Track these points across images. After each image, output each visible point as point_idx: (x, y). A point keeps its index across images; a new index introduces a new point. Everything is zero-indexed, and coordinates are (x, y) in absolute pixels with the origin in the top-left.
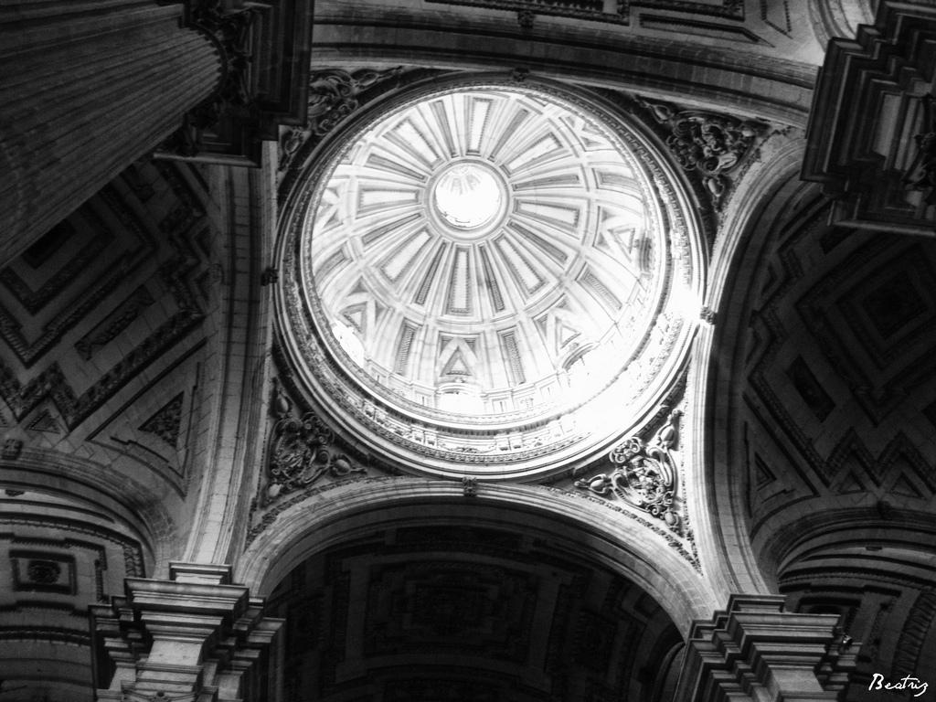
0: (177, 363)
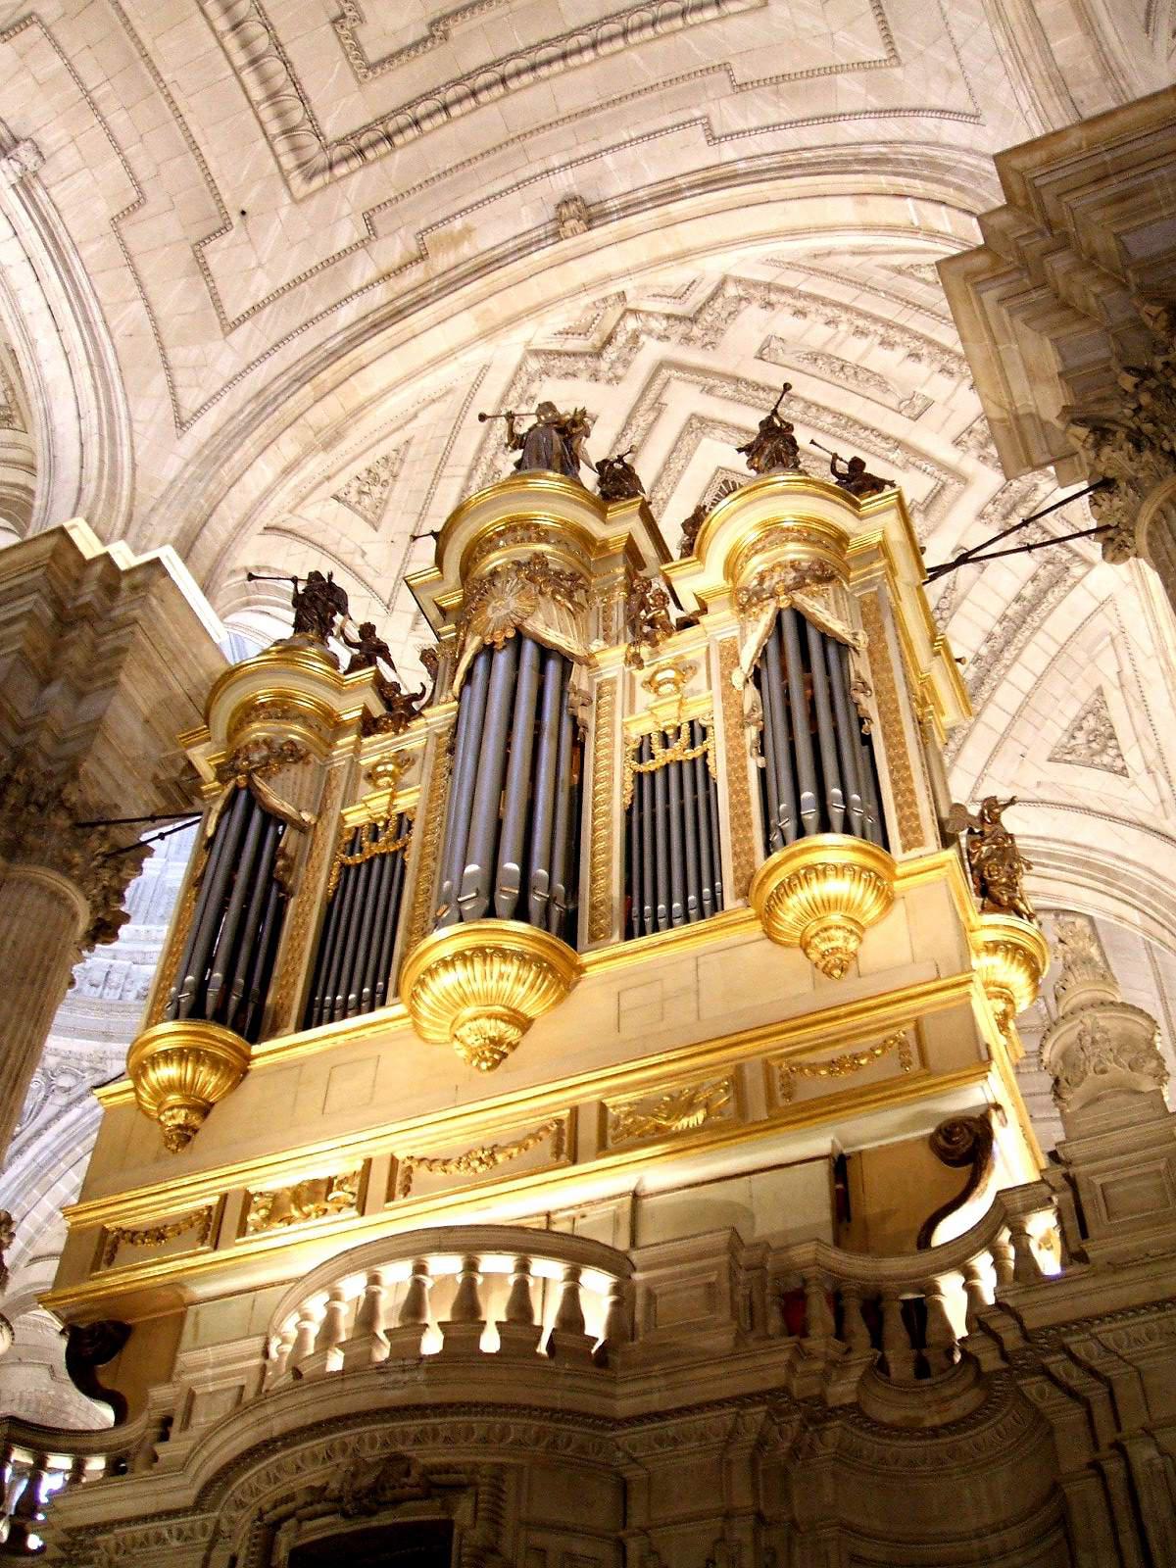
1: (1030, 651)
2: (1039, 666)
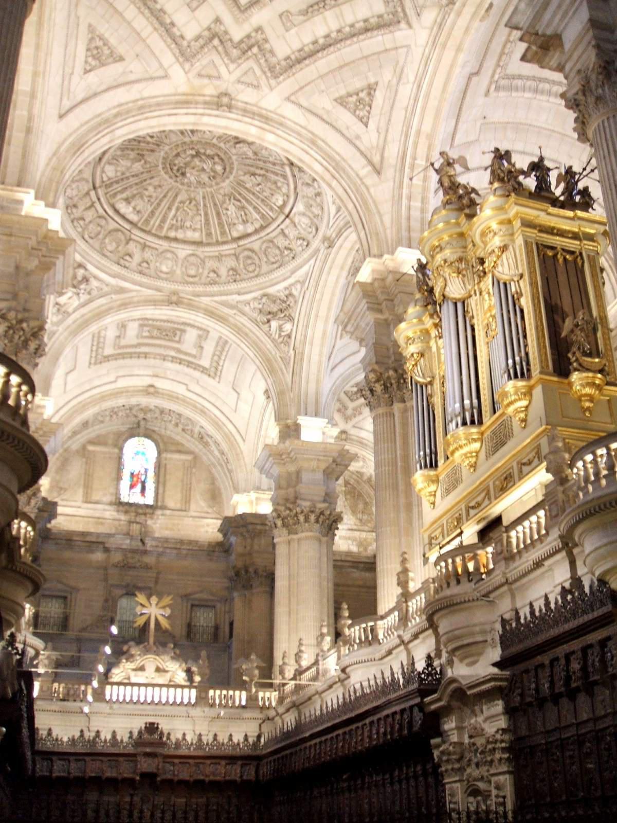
1: (144, 22)
2: (135, 24)
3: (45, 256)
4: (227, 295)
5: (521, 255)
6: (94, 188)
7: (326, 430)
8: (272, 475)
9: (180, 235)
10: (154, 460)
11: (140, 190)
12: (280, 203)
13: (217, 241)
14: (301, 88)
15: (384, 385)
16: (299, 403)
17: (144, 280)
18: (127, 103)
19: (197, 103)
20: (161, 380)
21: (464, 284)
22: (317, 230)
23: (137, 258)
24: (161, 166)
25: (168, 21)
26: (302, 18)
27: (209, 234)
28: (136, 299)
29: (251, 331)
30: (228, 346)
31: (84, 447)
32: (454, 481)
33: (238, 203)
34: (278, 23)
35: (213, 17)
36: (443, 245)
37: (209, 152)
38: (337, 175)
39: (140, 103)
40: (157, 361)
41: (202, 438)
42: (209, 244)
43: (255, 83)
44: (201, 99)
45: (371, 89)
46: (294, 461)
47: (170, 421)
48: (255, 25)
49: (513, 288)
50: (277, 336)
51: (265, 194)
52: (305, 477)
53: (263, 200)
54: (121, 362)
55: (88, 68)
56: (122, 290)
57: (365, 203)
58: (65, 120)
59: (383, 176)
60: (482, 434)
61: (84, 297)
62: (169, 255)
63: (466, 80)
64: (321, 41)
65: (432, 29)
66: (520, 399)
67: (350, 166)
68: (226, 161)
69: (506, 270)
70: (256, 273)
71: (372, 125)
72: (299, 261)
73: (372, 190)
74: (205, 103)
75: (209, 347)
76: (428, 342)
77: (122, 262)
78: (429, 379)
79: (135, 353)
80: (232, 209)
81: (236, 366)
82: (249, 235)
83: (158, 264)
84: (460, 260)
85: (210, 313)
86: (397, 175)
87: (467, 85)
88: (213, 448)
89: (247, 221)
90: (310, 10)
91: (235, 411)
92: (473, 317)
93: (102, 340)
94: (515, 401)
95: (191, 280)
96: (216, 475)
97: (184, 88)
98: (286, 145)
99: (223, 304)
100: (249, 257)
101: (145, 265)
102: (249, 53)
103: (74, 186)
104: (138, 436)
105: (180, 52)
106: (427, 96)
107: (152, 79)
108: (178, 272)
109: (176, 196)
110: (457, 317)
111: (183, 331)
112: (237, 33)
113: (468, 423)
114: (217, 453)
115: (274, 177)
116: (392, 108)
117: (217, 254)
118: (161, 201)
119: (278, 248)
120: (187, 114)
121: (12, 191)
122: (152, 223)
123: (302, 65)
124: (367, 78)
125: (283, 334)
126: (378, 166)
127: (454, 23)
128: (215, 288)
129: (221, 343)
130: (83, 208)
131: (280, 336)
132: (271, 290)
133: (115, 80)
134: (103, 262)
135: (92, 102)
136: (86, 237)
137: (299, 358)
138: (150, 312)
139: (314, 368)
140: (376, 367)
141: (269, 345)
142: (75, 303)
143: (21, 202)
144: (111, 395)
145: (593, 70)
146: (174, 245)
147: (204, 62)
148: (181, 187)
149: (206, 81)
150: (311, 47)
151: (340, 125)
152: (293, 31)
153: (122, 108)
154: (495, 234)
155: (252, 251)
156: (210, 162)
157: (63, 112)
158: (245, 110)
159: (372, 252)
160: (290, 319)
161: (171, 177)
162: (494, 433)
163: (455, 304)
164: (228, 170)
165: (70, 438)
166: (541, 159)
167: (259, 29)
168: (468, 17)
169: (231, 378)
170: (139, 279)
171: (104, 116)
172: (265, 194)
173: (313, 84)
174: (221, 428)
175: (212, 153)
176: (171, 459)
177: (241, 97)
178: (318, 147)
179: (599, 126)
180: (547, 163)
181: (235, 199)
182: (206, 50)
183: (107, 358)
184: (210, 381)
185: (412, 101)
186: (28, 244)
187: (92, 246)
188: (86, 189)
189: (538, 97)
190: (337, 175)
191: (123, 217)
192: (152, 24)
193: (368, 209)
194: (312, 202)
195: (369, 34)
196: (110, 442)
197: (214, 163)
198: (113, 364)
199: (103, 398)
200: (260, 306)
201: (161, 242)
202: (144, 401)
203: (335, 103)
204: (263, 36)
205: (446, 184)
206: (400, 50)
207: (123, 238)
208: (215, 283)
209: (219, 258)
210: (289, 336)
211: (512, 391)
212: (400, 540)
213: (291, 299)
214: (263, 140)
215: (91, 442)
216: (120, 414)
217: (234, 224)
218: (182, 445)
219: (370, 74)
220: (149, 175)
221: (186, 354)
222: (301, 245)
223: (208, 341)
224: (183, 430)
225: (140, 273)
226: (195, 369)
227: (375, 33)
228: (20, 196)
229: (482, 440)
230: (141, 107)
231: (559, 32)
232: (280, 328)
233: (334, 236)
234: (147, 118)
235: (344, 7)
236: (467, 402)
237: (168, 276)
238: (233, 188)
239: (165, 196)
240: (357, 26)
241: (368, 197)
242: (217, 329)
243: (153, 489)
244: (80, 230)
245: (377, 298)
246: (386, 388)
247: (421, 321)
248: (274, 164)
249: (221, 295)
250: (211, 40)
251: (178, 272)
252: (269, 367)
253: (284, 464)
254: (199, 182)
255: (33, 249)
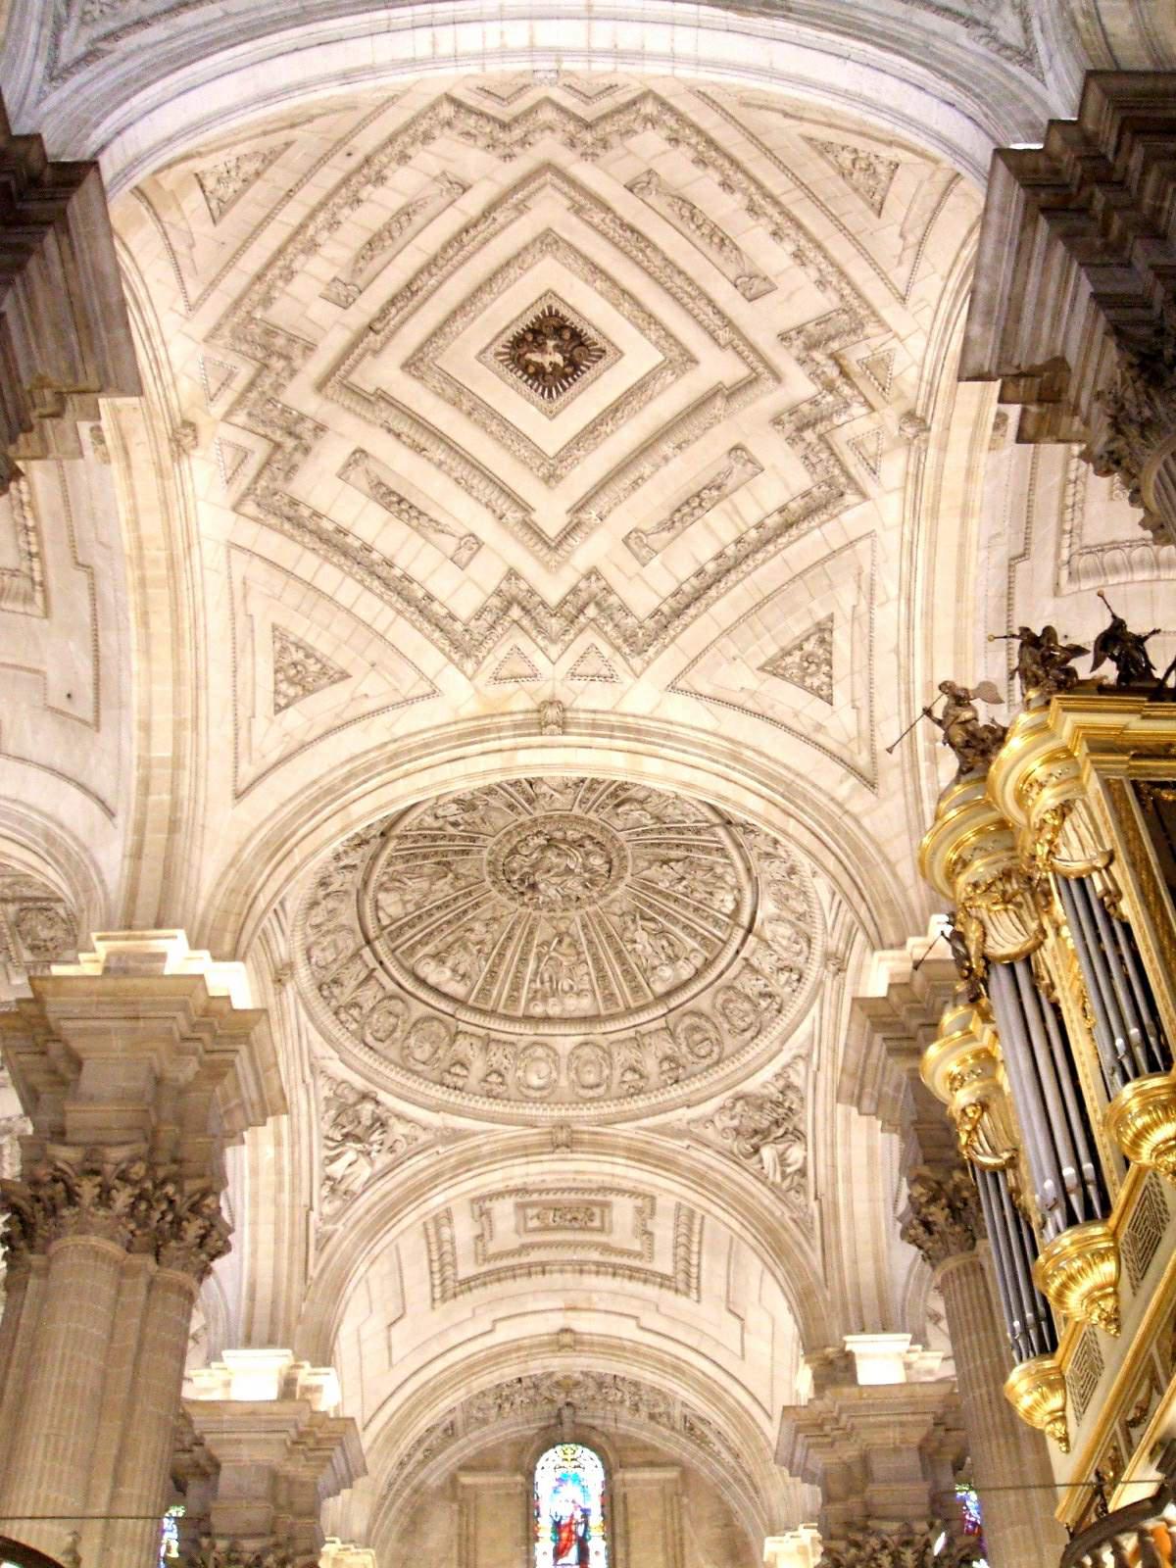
0: (753, 138)
3: (207, 1052)
4: (665, 1111)
5: (1102, 811)
6: (368, 942)
7: (913, 1357)
8: (814, 1475)
9: (554, 1009)
10: (600, 1490)
11: (458, 934)
12: (730, 906)
13: (628, 1008)
14: (694, 661)
15: (950, 1206)
16: (845, 1306)
17: (498, 1107)
18: (367, 752)
19: (500, 729)
20: (584, 1315)
21: (1022, 921)
22: (809, 941)
23: (478, 1067)
24: (488, 880)
25: (420, 594)
26: (666, 535)
27: (610, 998)
28: (485, 1149)
29: (727, 1177)
30: (697, 1222)
31: (453, 1480)
32: (1091, 1367)
33: (652, 925)
34: (624, 556)
35: (503, 570)
36: (967, 856)
37: (572, 835)
38: (792, 809)
39: (392, 747)
40: (568, 1276)
41: (692, 1429)
42: (612, 1017)
43: (605, 671)
44: (507, 719)
45: (823, 631)
46: (849, 1433)
47: (622, 1402)
48: (583, 567)
49: (1098, 884)
50: (778, 1179)
51: (697, 895)
52: (879, 1466)
53: (696, 909)
54: (495, 1289)
55: (282, 702)
56: (457, 1135)
57: (857, 848)
58: (247, 801)
59: (881, 790)
60: (1114, 1235)
61: (383, 1160)
62: (540, 1052)
63: (1005, 572)
64: (711, 567)
65: (905, 488)
66: (1156, 1124)
67: (814, 785)
68: (609, 846)
69: (1077, 853)
70: (715, 1056)
71: (840, 695)
72: (790, 1014)
73: (866, 822)
74: (516, 726)
75: (664, 1230)
76: (993, 1077)
77: (448, 1079)
78: (1006, 1155)
79: (521, 1266)
80: (642, 936)
81: (724, 1260)
82: (685, 985)
83: (520, 1073)
84: (1006, 875)
85: (639, 1155)
86: (908, 776)
87: (1010, 582)
88: (718, 1446)
89: (677, 958)
90: (678, 516)
91: (743, 1357)
92: (1052, 986)
93: (447, 1247)
94: (1146, 1130)
95: (591, 1093)
96: (734, 1505)
97: (471, 708)
98: (687, 774)
99: (662, 1130)
100: (695, 1029)
101: (494, 1078)
102: (582, 619)
103: (325, 942)
104: (562, 1443)
105: (452, 643)
106: (929, 614)
107: (408, 701)
108: (564, 1082)
109: (531, 932)
110: (1019, 995)
111: (605, 1205)
112: (553, 591)
113: (1080, 1218)
114: (725, 1455)
115: (706, 859)
116: (870, 656)
117: (631, 1033)
118: (504, 947)
119: (747, 997)
120: (483, 753)
121: (143, 938)
122: (495, 993)
123: (685, 619)
124: (810, 612)
125: (789, 1170)
126: (869, 776)
127: (940, 467)
128: (641, 1103)
129: (683, 1219)
130: (354, 983)
131: (784, 1176)
132: (750, 1086)
133: (338, 716)
134: (409, 1083)
135: (297, 761)
136: (369, 1039)
137: (829, 1215)
138: (520, 1172)
139: (864, 1229)
140: (925, 1171)
141: (766, 1198)
142: (364, 1171)
143: (161, 957)
144: (488, 1359)
145: (1124, 381)
146: (544, 1029)
147: (502, 652)
148: (536, 914)
149: (510, 687)
150: (694, 581)
151: (781, 713)
152: (655, 562)
153: (357, 763)
154: (1042, 786)
155: (699, 1014)
156: (578, 854)
157: (242, 786)
158: (594, 725)
159: (886, 941)
160: (798, 1135)
161: (512, 899)
162: (1134, 1227)
163: (1011, 968)
164: (616, 862)
165: (422, 1463)
166: (1118, 625)
167: (593, 573)
168: (965, 444)
169: (719, 1287)
170: (486, 1107)
171: (324, 783)
172: (697, 895)
173: (713, 650)
174: (720, 1399)
175: (577, 836)
176: (635, 1482)
177: (580, 703)
178: (745, 763)
179: (1159, 475)
180: (1134, 627)
181: (643, 918)
182: (499, 629)
183: (467, 1285)
184: (681, 1300)
185: (903, 632)
186: (170, 1031)
187: (386, 1058)
188: (352, 947)
189: (1165, 574)
190: (792, 809)
191: (435, 990)
192: (391, 605)
193: (863, 859)
194: (786, 890)
195: (794, 531)
196: (506, 1461)
197: (588, 854)
198: (479, 1294)
199: (471, 1368)
200: (736, 1122)
201: (517, 1028)
202: (559, 1364)
203: (765, 676)
204: (602, 583)
205: (958, 740)
206: (859, 546)
207: (443, 1032)
208: (640, 1091)
209: (638, 1041)
210: (802, 1172)
211: (1134, 1106)
212: (1040, 1554)
213: (791, 1095)
214: (642, 774)
215: (466, 1468)
216: (518, 1400)
217: (654, 968)
218: (655, 1449)
219: (814, 605)
220: (471, 901)
221: (622, 1252)
222: (788, 982)
223: (658, 1218)
224: (652, 1417)
225: (489, 1095)
226: (645, 1281)
227: (804, 526)
228: (156, 946)
229: (1116, 1252)
230: (395, 755)
231: (1058, 354)
232: (782, 1160)
233: (842, 946)
234: (406, 775)
235: (737, 497)
236: (1069, 1171)
237: (545, 1093)
238: (636, 897)
239: (509, 938)
240: (770, 522)
241: (860, 835)
242: (669, 1190)
243: (603, 1553)
244: (354, 1026)
245: (904, 1028)
246: (955, 1213)
247: (969, 1036)
248: (698, 832)
249: (654, 1114)
250: (506, 610)
251: (564, 1082)
252: (777, 1247)
253: (832, 1444)
254: (566, 898)
255: (185, 1039)
